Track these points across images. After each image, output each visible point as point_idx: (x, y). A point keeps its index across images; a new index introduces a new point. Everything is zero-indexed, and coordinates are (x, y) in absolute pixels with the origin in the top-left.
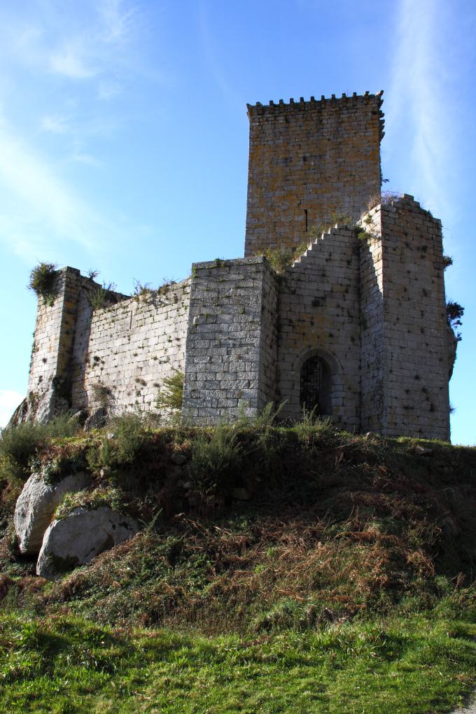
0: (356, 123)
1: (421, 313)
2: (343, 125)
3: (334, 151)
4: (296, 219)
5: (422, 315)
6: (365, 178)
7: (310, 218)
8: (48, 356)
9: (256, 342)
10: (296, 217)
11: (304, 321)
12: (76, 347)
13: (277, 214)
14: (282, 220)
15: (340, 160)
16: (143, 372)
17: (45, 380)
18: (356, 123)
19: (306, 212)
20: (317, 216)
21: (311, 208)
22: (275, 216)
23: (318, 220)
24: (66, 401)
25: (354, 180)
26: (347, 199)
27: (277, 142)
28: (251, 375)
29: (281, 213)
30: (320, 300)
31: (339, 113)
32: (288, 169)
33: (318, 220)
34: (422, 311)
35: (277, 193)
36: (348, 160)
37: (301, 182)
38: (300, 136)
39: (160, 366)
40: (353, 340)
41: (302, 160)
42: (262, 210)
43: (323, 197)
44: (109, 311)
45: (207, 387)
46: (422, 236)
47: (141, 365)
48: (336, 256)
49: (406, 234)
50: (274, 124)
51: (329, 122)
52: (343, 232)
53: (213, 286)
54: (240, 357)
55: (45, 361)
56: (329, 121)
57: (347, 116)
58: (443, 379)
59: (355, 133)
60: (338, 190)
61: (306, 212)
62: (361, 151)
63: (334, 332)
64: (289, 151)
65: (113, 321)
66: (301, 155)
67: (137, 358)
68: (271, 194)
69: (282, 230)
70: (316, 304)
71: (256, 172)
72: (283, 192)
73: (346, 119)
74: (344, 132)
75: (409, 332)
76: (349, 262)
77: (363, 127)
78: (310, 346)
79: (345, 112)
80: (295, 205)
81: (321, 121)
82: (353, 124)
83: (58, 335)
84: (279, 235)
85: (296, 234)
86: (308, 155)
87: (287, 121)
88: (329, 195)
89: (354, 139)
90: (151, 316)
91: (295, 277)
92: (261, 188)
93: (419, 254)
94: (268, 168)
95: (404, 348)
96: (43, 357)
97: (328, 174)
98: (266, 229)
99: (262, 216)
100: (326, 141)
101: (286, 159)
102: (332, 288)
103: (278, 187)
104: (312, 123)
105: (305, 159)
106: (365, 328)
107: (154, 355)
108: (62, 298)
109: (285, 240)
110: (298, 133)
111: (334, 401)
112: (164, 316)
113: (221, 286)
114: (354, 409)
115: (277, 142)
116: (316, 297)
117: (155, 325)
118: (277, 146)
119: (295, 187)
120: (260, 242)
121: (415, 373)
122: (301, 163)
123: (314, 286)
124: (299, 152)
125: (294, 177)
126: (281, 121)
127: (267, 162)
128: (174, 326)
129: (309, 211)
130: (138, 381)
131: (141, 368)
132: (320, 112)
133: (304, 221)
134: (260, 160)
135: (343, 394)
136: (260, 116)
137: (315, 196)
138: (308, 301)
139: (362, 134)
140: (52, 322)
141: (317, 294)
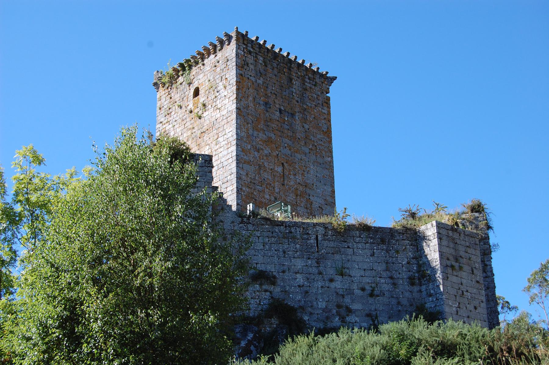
15: (306, 126)
16: (347, 300)
19: (283, 164)
29: (265, 158)
33: (292, 177)
39: (371, 300)
53: (452, 245)
54: (475, 308)
57: (309, 85)
61: (283, 164)
62: (320, 125)
64: (268, 97)
65: (284, 238)
67: (333, 285)
68: (256, 133)
71: (242, 103)
79: (308, 81)
80: (275, 154)
81: (291, 80)
85: (277, 184)
86: (282, 108)
90: (348, 247)
92: (248, 124)
94: (252, 105)
105: (280, 111)
107: (360, 286)
112: (369, 252)
115: (259, 81)
126: (260, 62)
128: (384, 265)
129: (286, 165)
130: (339, 306)
131: (343, 296)
137: (289, 152)
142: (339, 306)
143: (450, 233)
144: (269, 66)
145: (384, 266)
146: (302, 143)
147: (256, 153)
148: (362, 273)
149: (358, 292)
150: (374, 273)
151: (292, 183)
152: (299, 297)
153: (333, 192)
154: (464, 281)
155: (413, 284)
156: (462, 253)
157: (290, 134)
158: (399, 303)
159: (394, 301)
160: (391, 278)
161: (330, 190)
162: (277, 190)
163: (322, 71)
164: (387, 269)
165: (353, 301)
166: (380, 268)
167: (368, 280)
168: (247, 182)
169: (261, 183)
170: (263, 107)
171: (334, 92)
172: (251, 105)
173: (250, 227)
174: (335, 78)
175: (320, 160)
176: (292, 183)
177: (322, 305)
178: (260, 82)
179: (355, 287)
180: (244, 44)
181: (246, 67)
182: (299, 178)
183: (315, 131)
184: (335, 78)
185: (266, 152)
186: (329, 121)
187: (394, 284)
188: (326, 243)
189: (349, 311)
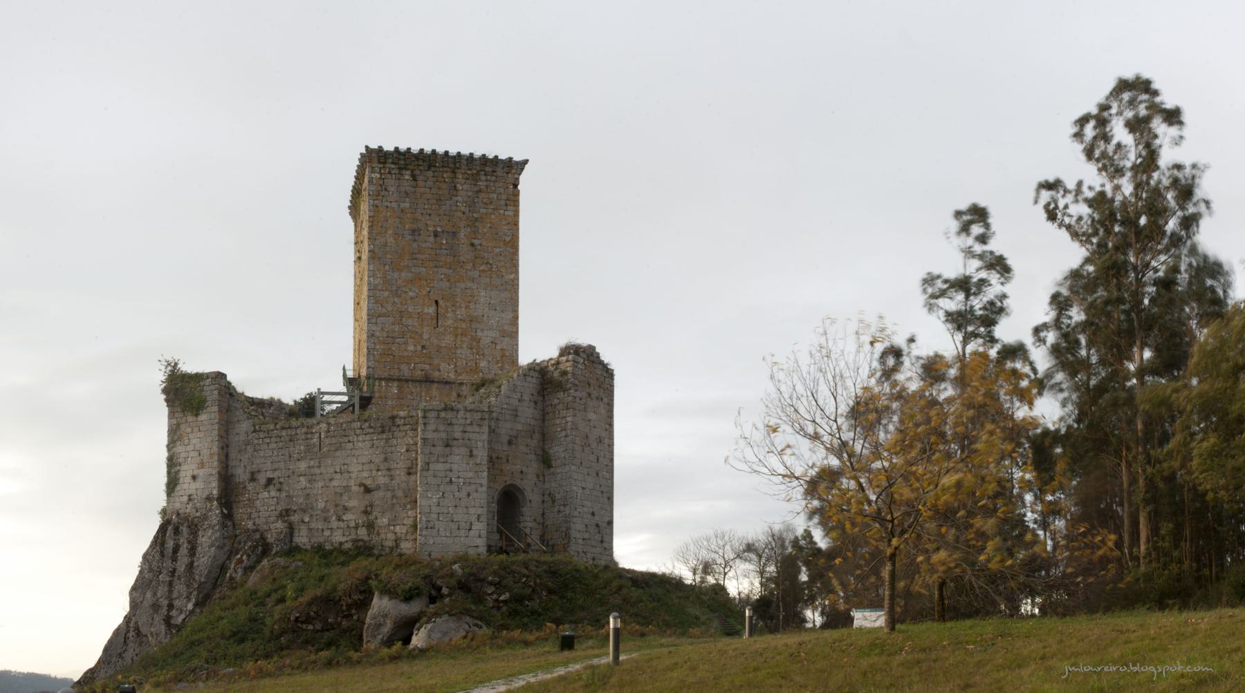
2: (482, 195)
8: (201, 473)
12: (231, 463)
14: (410, 309)
16: (345, 497)
19: (437, 302)
25: (491, 269)
27: (402, 205)
28: (480, 511)
31: (475, 178)
32: (415, 245)
35: (403, 274)
37: (431, 264)
40: (538, 476)
42: (386, 294)
44: (283, 428)
47: (338, 490)
48: (526, 398)
51: (464, 187)
52: (532, 373)
53: (442, 428)
54: (469, 495)
55: (194, 478)
60: (473, 280)
61: (437, 302)
63: (524, 469)
68: (396, 275)
69: (410, 322)
70: (510, 443)
71: (377, 242)
76: (536, 403)
77: (503, 202)
79: (483, 178)
80: (424, 292)
83: (215, 449)
85: (425, 329)
87: (414, 177)
88: (463, 286)
96: (189, 473)
97: (462, 259)
98: (391, 319)
100: (460, 214)
101: (414, 231)
104: (444, 186)
105: (436, 235)
106: (550, 466)
108: (215, 409)
112: (368, 444)
113: (449, 429)
115: (402, 205)
117: (357, 453)
120: (385, 335)
122: (432, 239)
123: (508, 425)
127: (390, 232)
129: (441, 302)
132: (453, 172)
133: (434, 315)
137: (448, 284)
138: (505, 439)
140: (199, 435)
142: (336, 506)
143: (443, 414)
144: (420, 178)
145: (383, 456)
146: (469, 266)
147: (396, 300)
148: (360, 468)
149: (355, 489)
150: (372, 466)
151: (450, 322)
152: (301, 500)
153: (516, 318)
154: (455, 467)
155: (409, 474)
156: (458, 435)
157: (450, 259)
158: (393, 497)
159: (389, 494)
160: (389, 470)
161: (510, 315)
162: (426, 336)
163: (503, 156)
164: (386, 460)
165: (350, 499)
166: (378, 459)
167: (365, 474)
169: (403, 335)
170: (409, 237)
171: (526, 181)
172: (391, 240)
173: (262, 435)
174: (526, 162)
176: (450, 322)
177: (321, 505)
178: (408, 205)
179: (352, 483)
181: (383, 193)
182: (461, 313)
184: (526, 162)
185: (411, 294)
186: (516, 224)
188: (327, 441)
189: (346, 509)
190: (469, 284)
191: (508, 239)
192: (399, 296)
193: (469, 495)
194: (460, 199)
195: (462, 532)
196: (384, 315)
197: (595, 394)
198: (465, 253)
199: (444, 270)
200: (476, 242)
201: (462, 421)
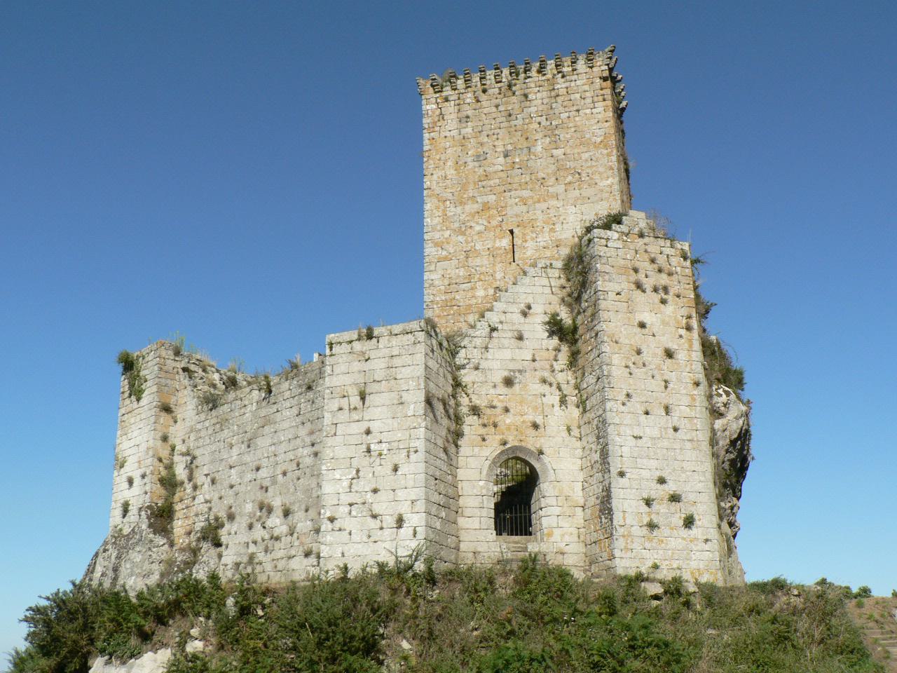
0: (578, 96)
1: (663, 383)
2: (560, 99)
3: (548, 140)
4: (498, 244)
5: (666, 387)
6: (597, 177)
7: (518, 241)
9: (420, 444)
10: (497, 241)
11: (494, 407)
13: (470, 239)
15: (558, 153)
17: (133, 510)
18: (578, 96)
20: (528, 237)
21: (518, 226)
22: (467, 242)
23: (530, 244)
24: (165, 541)
26: (573, 209)
29: (476, 237)
30: (517, 374)
34: (666, 381)
36: (568, 152)
38: (498, 120)
41: (502, 155)
42: (447, 234)
43: (535, 210)
45: (354, 513)
46: (660, 271)
49: (636, 270)
50: (459, 105)
56: (539, 95)
58: (702, 479)
59: (578, 111)
60: (557, 197)
61: (512, 232)
62: (587, 136)
63: (539, 420)
64: (482, 144)
66: (500, 149)
68: (459, 210)
69: (478, 261)
70: (509, 382)
72: (476, 206)
73: (562, 91)
74: (561, 109)
75: (647, 413)
77: (589, 100)
78: (505, 443)
80: (494, 223)
81: (526, 96)
82: (572, 97)
84: (473, 270)
85: (499, 267)
86: (509, 147)
88: (544, 206)
89: (577, 119)
91: (478, 343)
93: (656, 298)
95: (641, 438)
97: (541, 175)
98: (454, 262)
99: (448, 243)
102: (534, 355)
103: (469, 198)
109: (482, 277)
110: (494, 115)
111: (545, 522)
114: (576, 531)
115: (463, 131)
116: (511, 370)
118: (464, 138)
119: (494, 197)
121: (658, 474)
122: (501, 160)
123: (507, 354)
124: (496, 143)
125: (491, 183)
126: (468, 101)
127: (449, 163)
134: (440, 160)
135: (557, 511)
136: (438, 95)
137: (524, 208)
138: (498, 377)
139: (588, 111)
141: (512, 366)
154: (375, 426)
162: (499, 275)
168: (443, 288)
172: (451, 172)
175: (588, 192)
180: (435, 93)
182: (544, 239)
183: (576, 151)
185: (478, 228)
187: (316, 454)
190: (553, 202)
191: (599, 140)
192: (463, 234)
193: (396, 469)
194: (533, 109)
195: (387, 532)
196: (446, 259)
197: (648, 284)
198: (543, 166)
199: (519, 193)
200: (555, 152)
201: (387, 352)
